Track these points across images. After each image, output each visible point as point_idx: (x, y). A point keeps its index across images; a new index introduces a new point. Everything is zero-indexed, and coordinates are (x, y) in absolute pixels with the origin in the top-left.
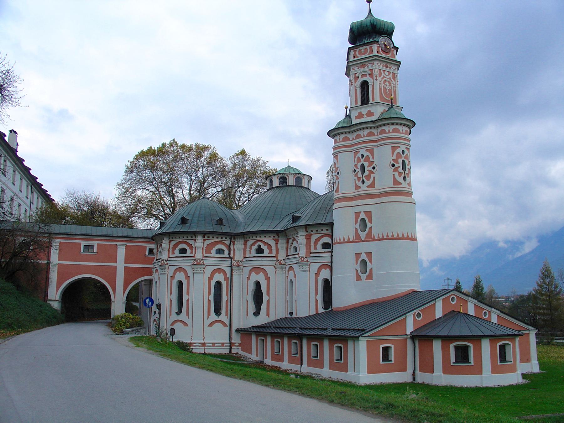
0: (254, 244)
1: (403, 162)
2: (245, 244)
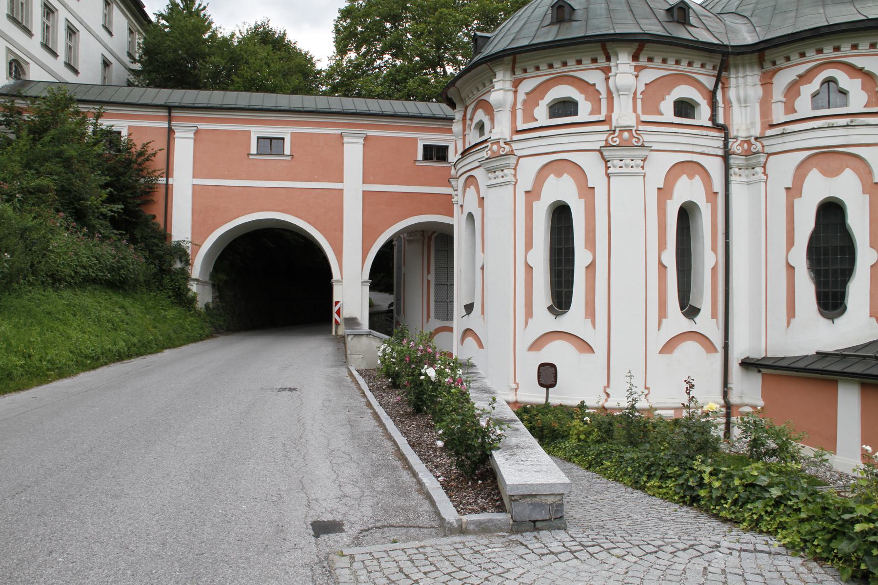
0: (803, 78)
2: (767, 83)
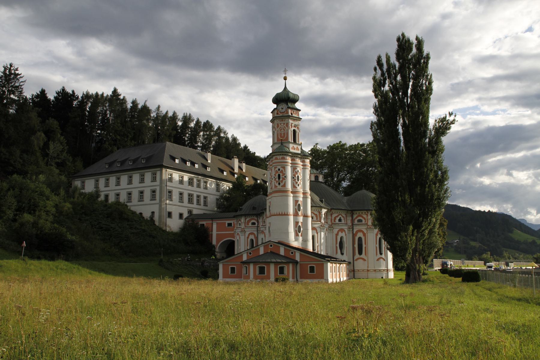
1: (279, 176)
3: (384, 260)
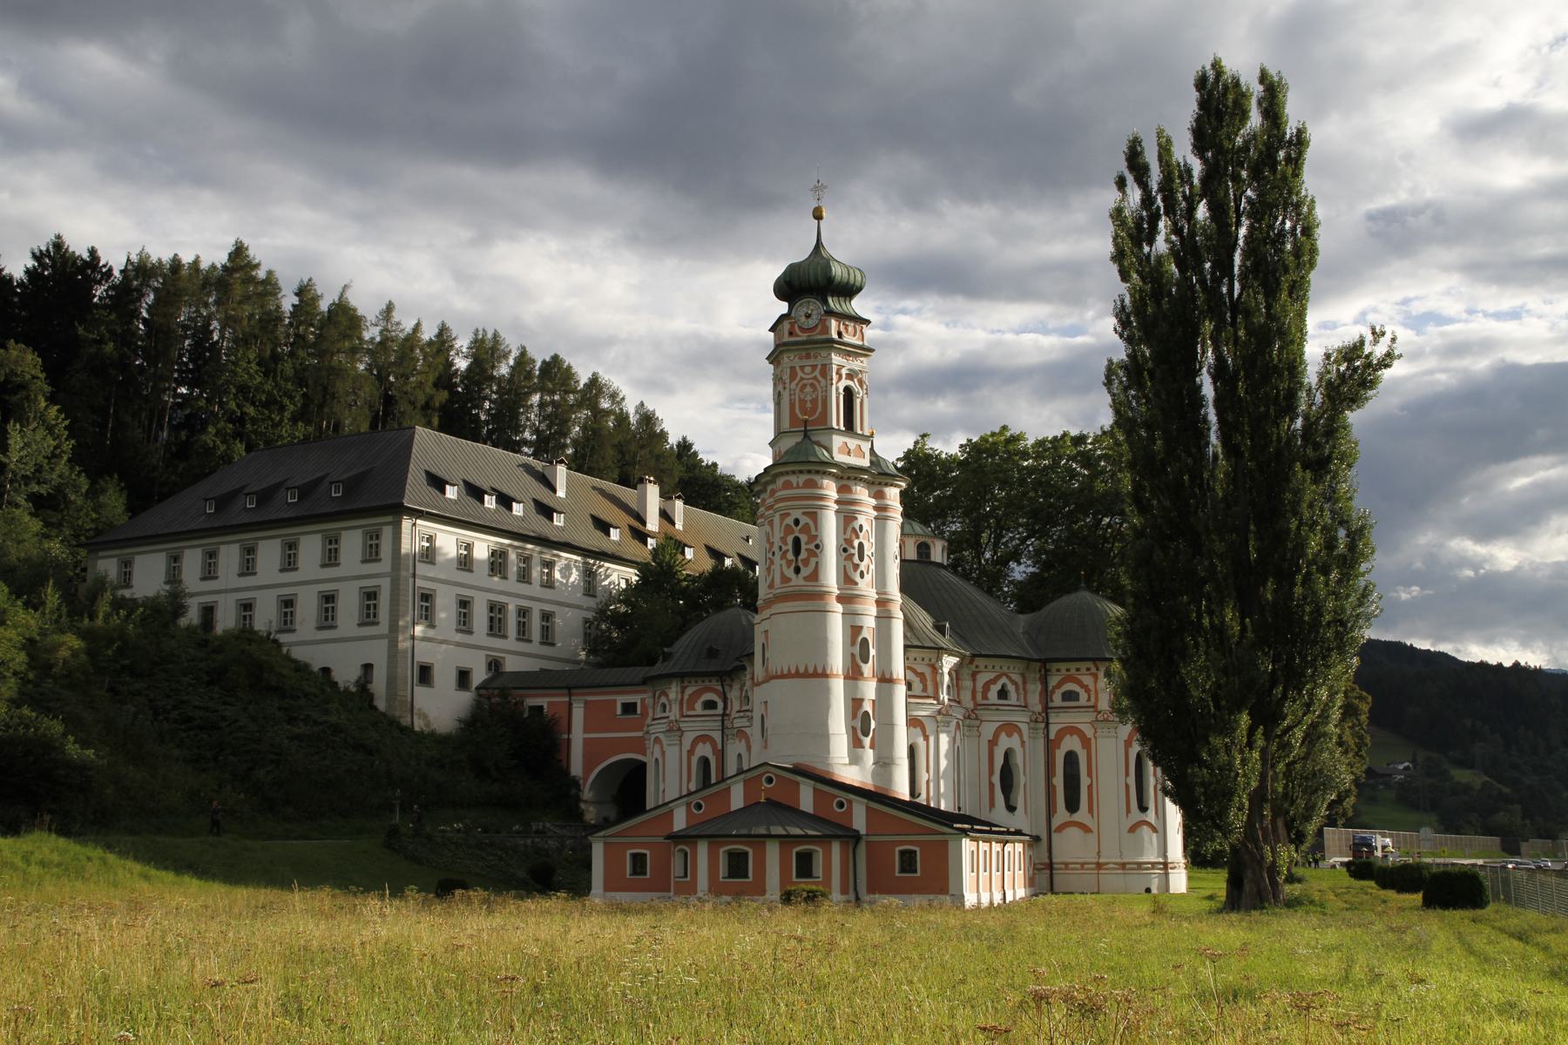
1: (797, 542)
3: (1155, 830)
